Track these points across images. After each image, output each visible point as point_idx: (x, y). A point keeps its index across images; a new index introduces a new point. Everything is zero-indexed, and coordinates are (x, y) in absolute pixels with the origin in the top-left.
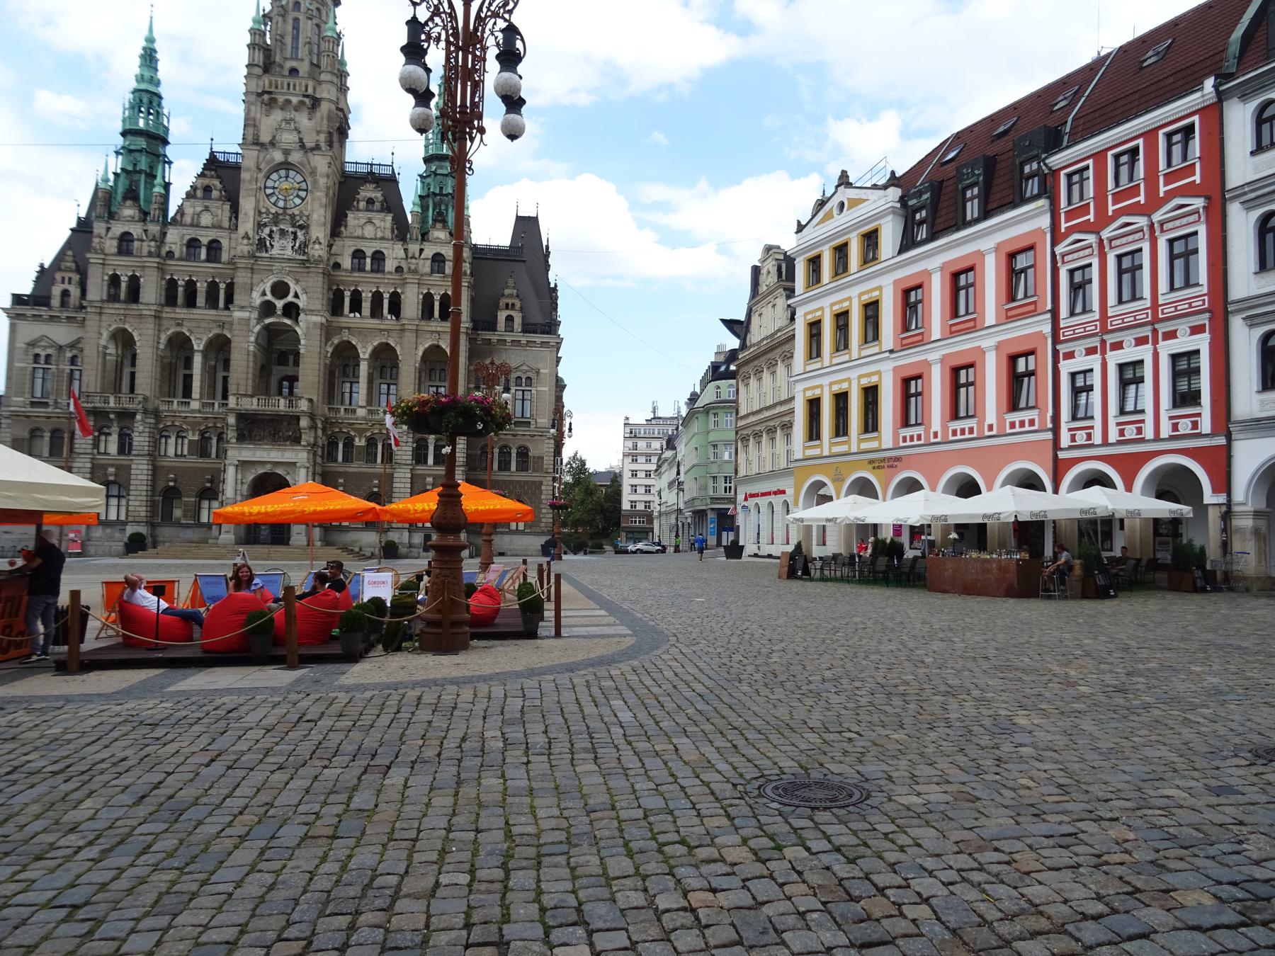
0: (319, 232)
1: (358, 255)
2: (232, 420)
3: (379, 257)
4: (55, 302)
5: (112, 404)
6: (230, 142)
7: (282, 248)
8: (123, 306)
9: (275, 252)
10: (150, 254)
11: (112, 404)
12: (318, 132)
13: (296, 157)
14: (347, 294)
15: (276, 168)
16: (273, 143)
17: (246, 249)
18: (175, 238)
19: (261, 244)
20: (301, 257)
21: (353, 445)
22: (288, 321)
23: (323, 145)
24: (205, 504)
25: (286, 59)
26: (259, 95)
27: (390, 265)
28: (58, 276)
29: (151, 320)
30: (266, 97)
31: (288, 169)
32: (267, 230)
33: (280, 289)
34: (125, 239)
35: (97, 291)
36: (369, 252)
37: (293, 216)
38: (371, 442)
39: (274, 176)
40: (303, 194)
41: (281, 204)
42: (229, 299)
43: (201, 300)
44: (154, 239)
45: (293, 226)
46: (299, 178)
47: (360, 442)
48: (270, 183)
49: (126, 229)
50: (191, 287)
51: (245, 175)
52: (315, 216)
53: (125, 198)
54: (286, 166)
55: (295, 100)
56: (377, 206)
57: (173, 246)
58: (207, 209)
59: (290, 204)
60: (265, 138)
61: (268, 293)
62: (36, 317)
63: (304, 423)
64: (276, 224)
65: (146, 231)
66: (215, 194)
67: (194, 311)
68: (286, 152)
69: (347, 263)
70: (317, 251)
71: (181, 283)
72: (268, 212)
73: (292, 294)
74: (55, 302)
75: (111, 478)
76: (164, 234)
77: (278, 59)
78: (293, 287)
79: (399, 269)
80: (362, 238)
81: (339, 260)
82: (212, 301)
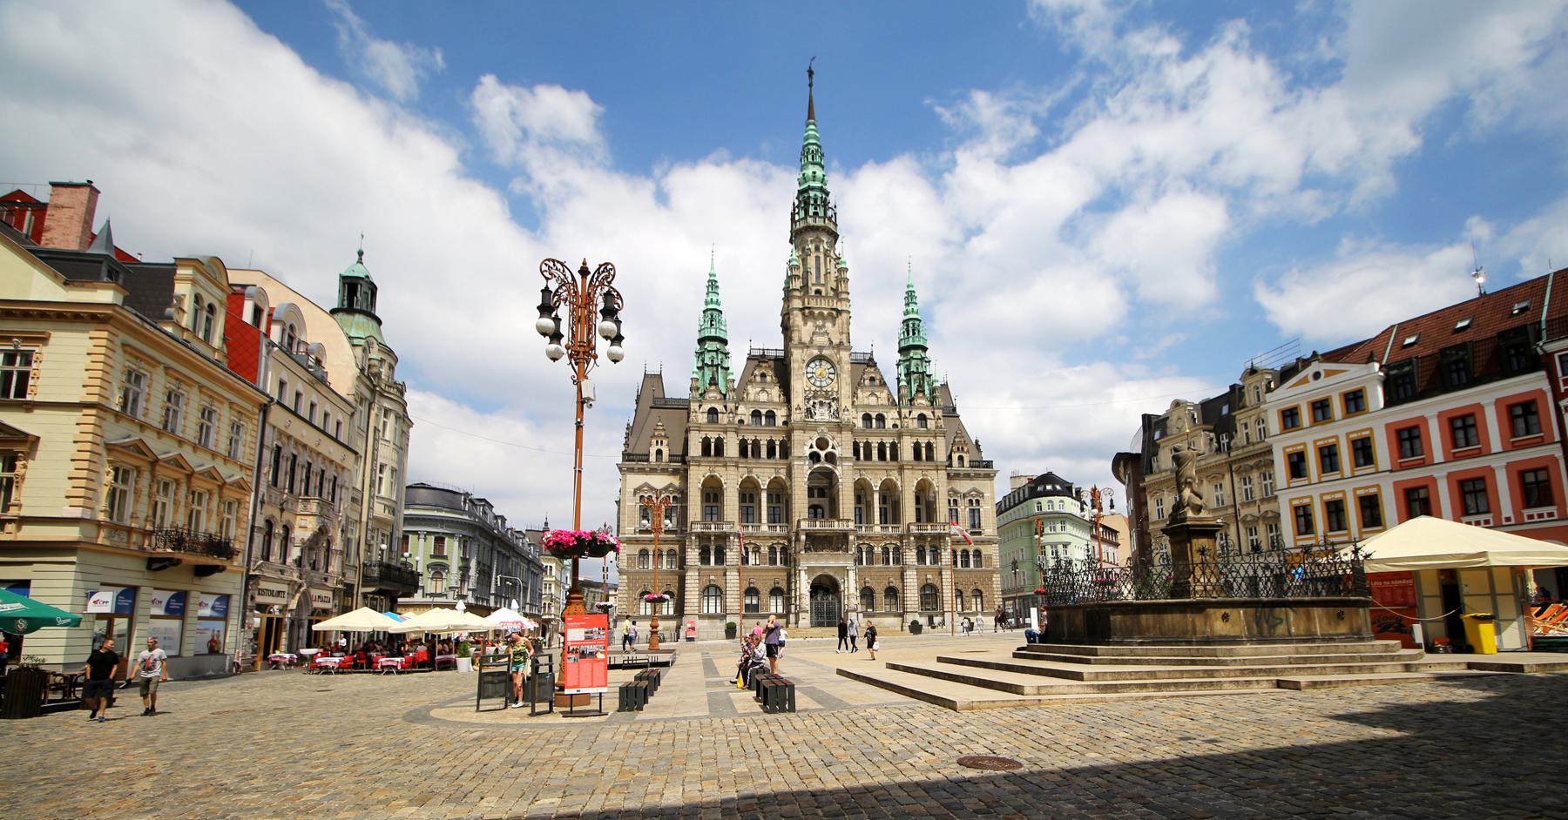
0: (846, 402)
1: (867, 418)
2: (803, 537)
3: (881, 418)
4: (653, 458)
5: (713, 530)
6: (774, 343)
7: (822, 414)
8: (715, 459)
9: (817, 417)
10: (729, 422)
11: (713, 530)
12: (842, 333)
13: (825, 352)
14: (861, 445)
15: (812, 360)
16: (811, 341)
17: (799, 416)
18: (744, 412)
19: (809, 413)
20: (835, 420)
21: (873, 553)
22: (830, 466)
23: (845, 341)
24: (773, 601)
25: (813, 285)
26: (801, 310)
27: (889, 424)
28: (654, 441)
29: (733, 468)
30: (807, 311)
31: (821, 360)
32: (811, 402)
33: (822, 444)
34: (713, 411)
35: (695, 450)
36: (874, 415)
37: (827, 392)
38: (886, 550)
39: (812, 365)
40: (832, 376)
41: (818, 384)
42: (786, 452)
43: (764, 453)
44: (731, 412)
45: (828, 399)
46: (829, 366)
47: (878, 550)
48: (809, 370)
49: (713, 405)
50: (756, 443)
51: (794, 365)
52: (843, 392)
53: (710, 384)
54: (820, 358)
55: (826, 312)
56: (877, 382)
57: (743, 418)
58: (763, 390)
59: (824, 384)
60: (806, 339)
61: (815, 446)
62: (642, 471)
63: (851, 538)
64: (814, 397)
65: (725, 407)
66: (768, 379)
67: (761, 461)
68: (821, 348)
69: (859, 423)
70: (845, 417)
71: (750, 442)
72: (810, 390)
73: (830, 447)
74: (653, 458)
75: (712, 583)
76: (737, 408)
77: (810, 285)
78: (831, 443)
79: (895, 426)
80: (869, 406)
81: (855, 421)
82: (771, 453)
